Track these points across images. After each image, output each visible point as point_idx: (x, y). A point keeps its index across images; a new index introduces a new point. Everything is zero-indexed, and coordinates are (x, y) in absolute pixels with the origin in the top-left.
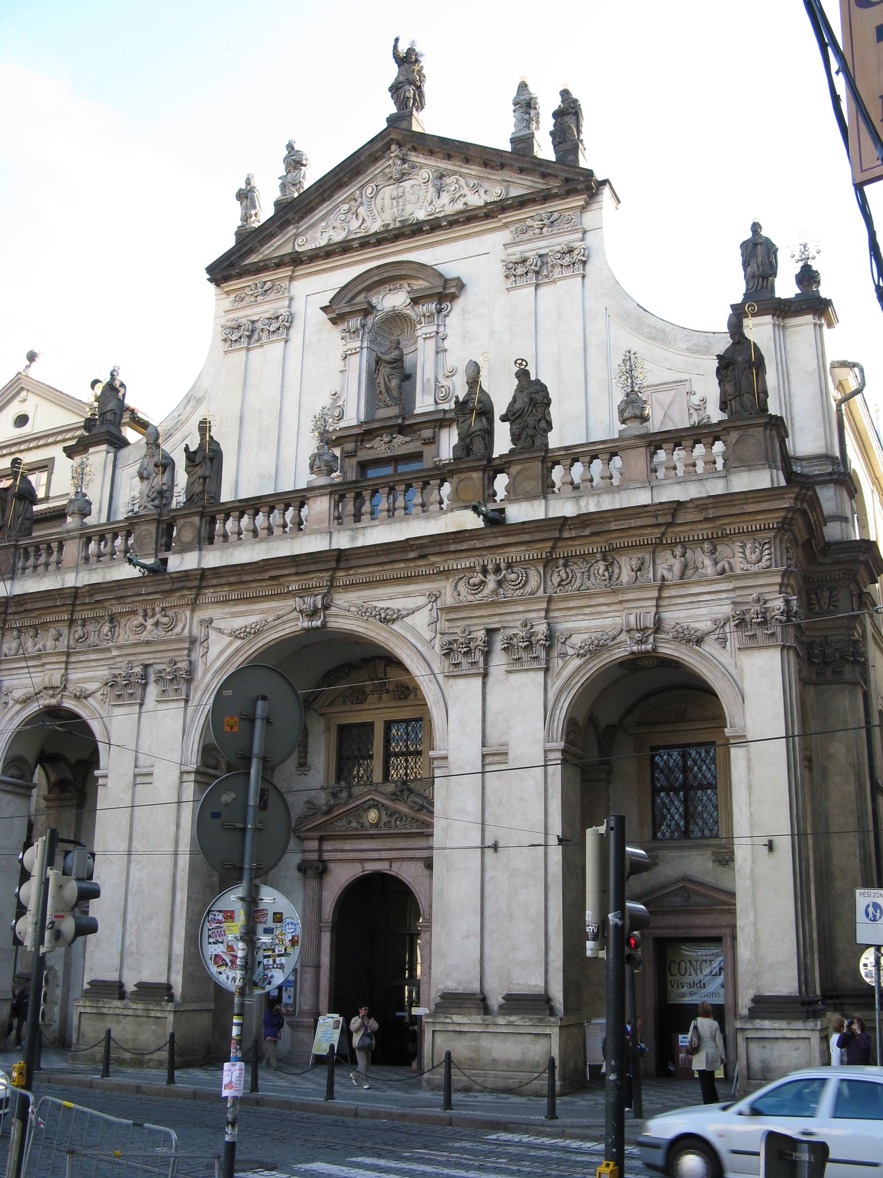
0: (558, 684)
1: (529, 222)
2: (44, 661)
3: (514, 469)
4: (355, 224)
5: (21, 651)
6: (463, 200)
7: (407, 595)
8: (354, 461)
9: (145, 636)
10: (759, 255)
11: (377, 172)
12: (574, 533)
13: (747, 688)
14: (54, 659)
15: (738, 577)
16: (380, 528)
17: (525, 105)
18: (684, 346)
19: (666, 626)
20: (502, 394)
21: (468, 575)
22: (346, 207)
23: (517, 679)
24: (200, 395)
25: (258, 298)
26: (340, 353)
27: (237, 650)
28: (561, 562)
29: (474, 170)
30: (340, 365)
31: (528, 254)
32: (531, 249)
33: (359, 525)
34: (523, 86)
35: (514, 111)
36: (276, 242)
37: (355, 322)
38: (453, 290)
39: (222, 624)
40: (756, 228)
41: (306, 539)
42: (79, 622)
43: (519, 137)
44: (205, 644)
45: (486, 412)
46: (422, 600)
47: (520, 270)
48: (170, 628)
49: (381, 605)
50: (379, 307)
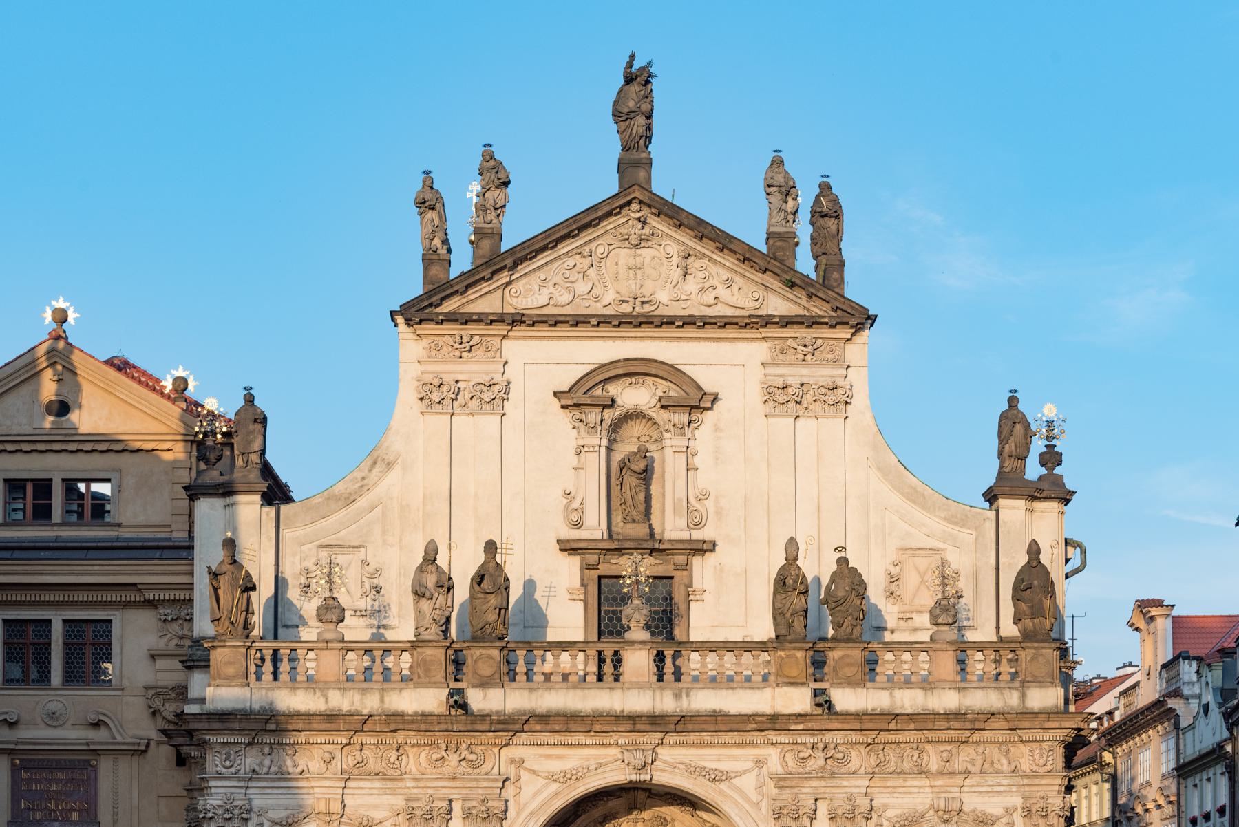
1: (790, 342)
2: (313, 784)
5: (273, 769)
6: (714, 294)
7: (735, 758)
8: (595, 574)
9: (446, 770)
11: (609, 227)
12: (899, 726)
14: (327, 783)
15: (1029, 777)
16: (706, 691)
19: (965, 808)
21: (800, 748)
22: (571, 262)
24: (391, 458)
25: (465, 354)
26: (573, 444)
27: (557, 794)
28: (881, 747)
29: (729, 260)
30: (574, 460)
31: (790, 380)
32: (794, 375)
33: (680, 685)
34: (778, 163)
36: (485, 287)
37: (594, 416)
38: (709, 405)
39: (535, 768)
42: (358, 747)
43: (779, 233)
44: (518, 784)
46: (750, 764)
48: (475, 765)
49: (709, 765)
50: (619, 401)
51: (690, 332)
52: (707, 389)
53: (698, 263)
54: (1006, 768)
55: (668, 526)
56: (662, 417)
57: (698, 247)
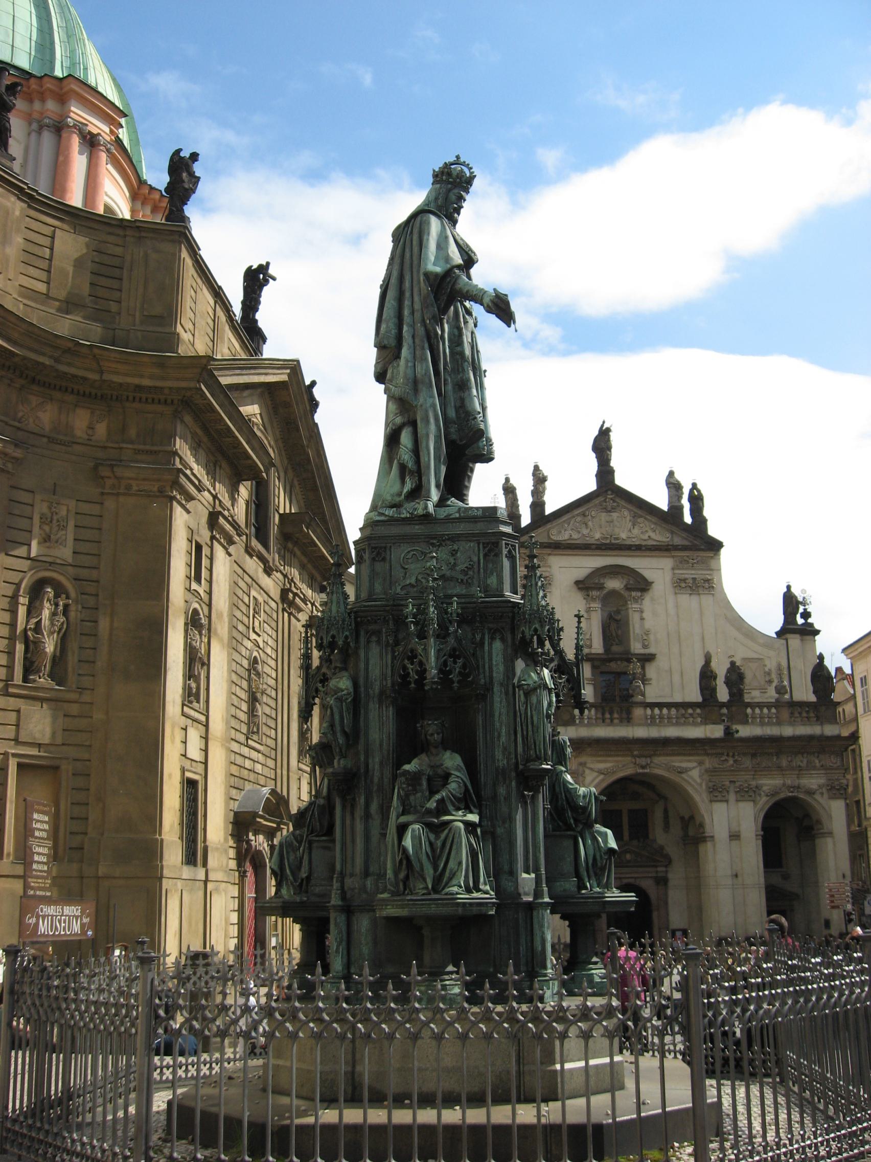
0: (758, 806)
3: (734, 709)
4: (585, 532)
7: (689, 761)
10: (791, 603)
13: (833, 814)
17: (674, 486)
18: (761, 641)
20: (720, 668)
22: (579, 519)
23: (741, 804)
27: (603, 780)
29: (654, 519)
31: (686, 576)
32: (688, 574)
34: (671, 474)
35: (668, 488)
36: (540, 530)
37: (595, 593)
39: (592, 766)
40: (789, 587)
41: (636, 728)
45: (715, 678)
46: (695, 764)
47: (683, 585)
49: (677, 764)
51: (638, 553)
52: (650, 580)
53: (639, 520)
54: (818, 765)
55: (632, 647)
56: (626, 594)
57: (640, 512)
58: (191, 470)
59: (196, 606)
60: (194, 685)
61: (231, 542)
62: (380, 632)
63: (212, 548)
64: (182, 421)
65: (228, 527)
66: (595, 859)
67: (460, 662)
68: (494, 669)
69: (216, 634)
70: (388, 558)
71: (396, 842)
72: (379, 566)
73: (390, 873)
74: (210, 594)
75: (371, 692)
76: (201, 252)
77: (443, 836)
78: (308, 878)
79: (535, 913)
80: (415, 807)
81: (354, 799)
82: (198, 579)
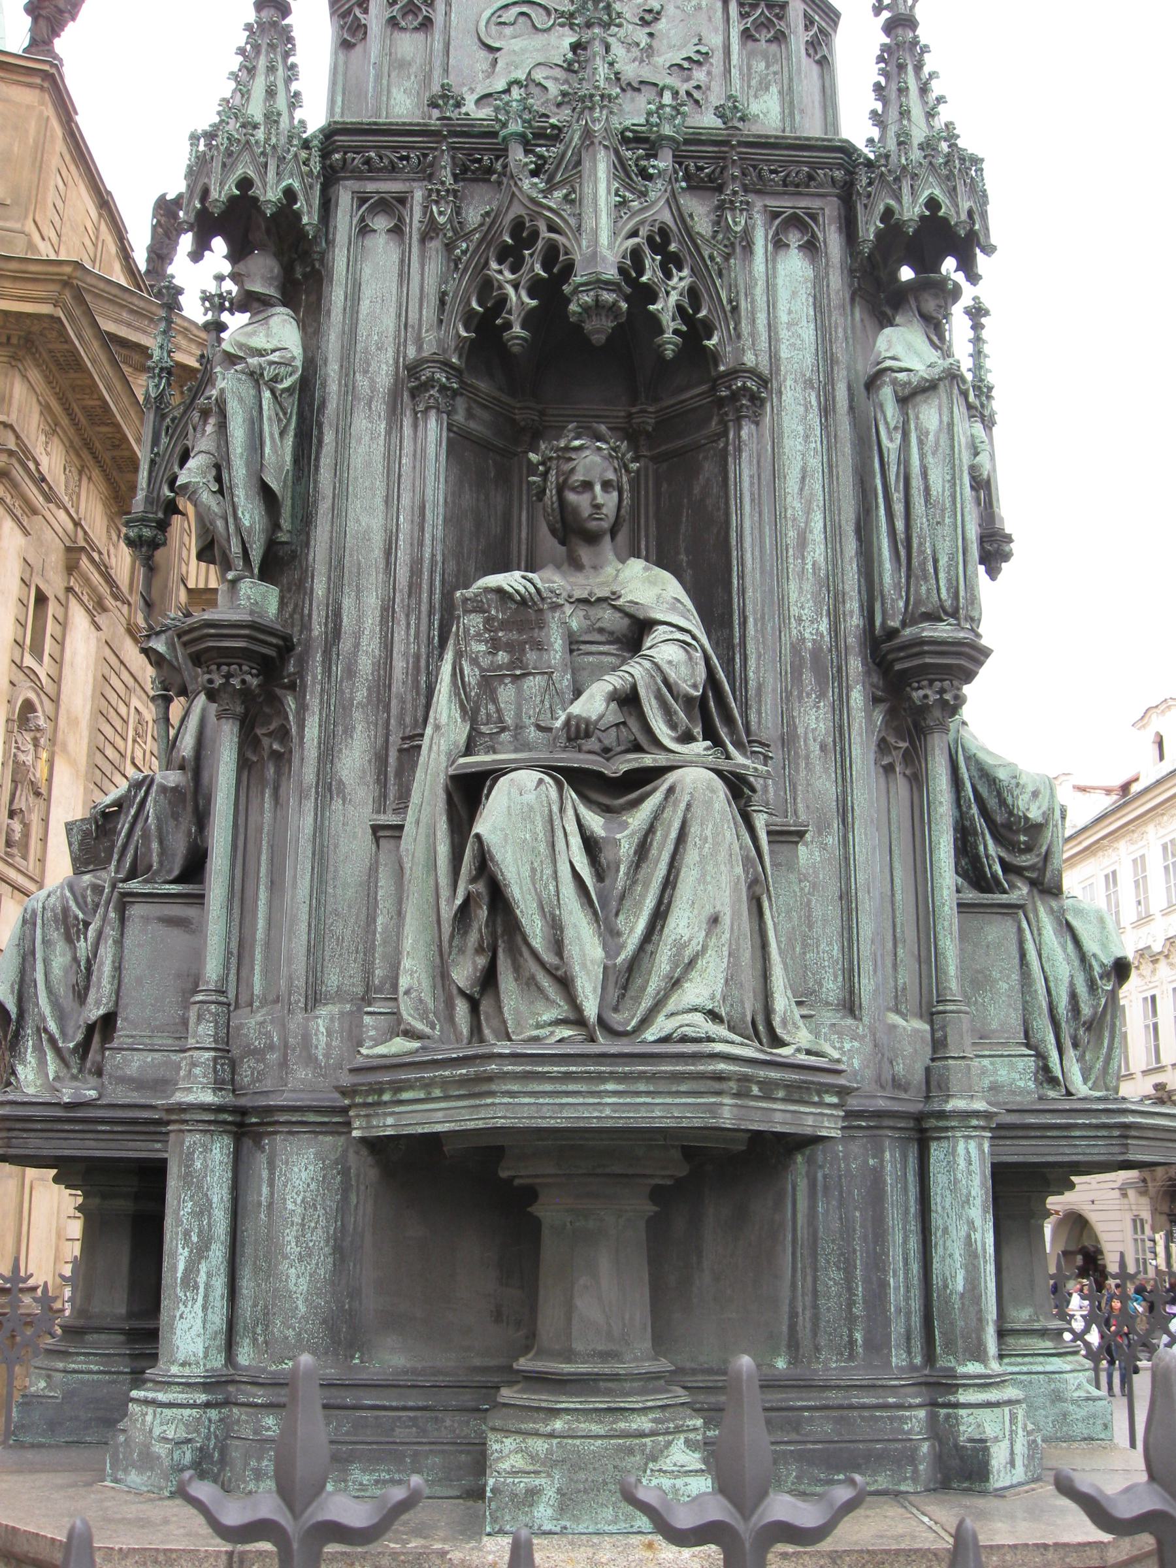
58: (37, 464)
59: (32, 696)
60: (17, 826)
61: (101, 607)
62: (402, 200)
63: (65, 606)
64: (24, 377)
65: (96, 578)
66: (1073, 996)
67: (681, 280)
68: (784, 334)
69: (65, 749)
70: (439, 19)
71: (443, 850)
72: (409, 44)
73: (414, 973)
74: (57, 681)
75: (362, 382)
76: (78, 119)
77: (638, 819)
78: (108, 1022)
79: (937, 1152)
80: (519, 727)
81: (283, 734)
82: (37, 651)
